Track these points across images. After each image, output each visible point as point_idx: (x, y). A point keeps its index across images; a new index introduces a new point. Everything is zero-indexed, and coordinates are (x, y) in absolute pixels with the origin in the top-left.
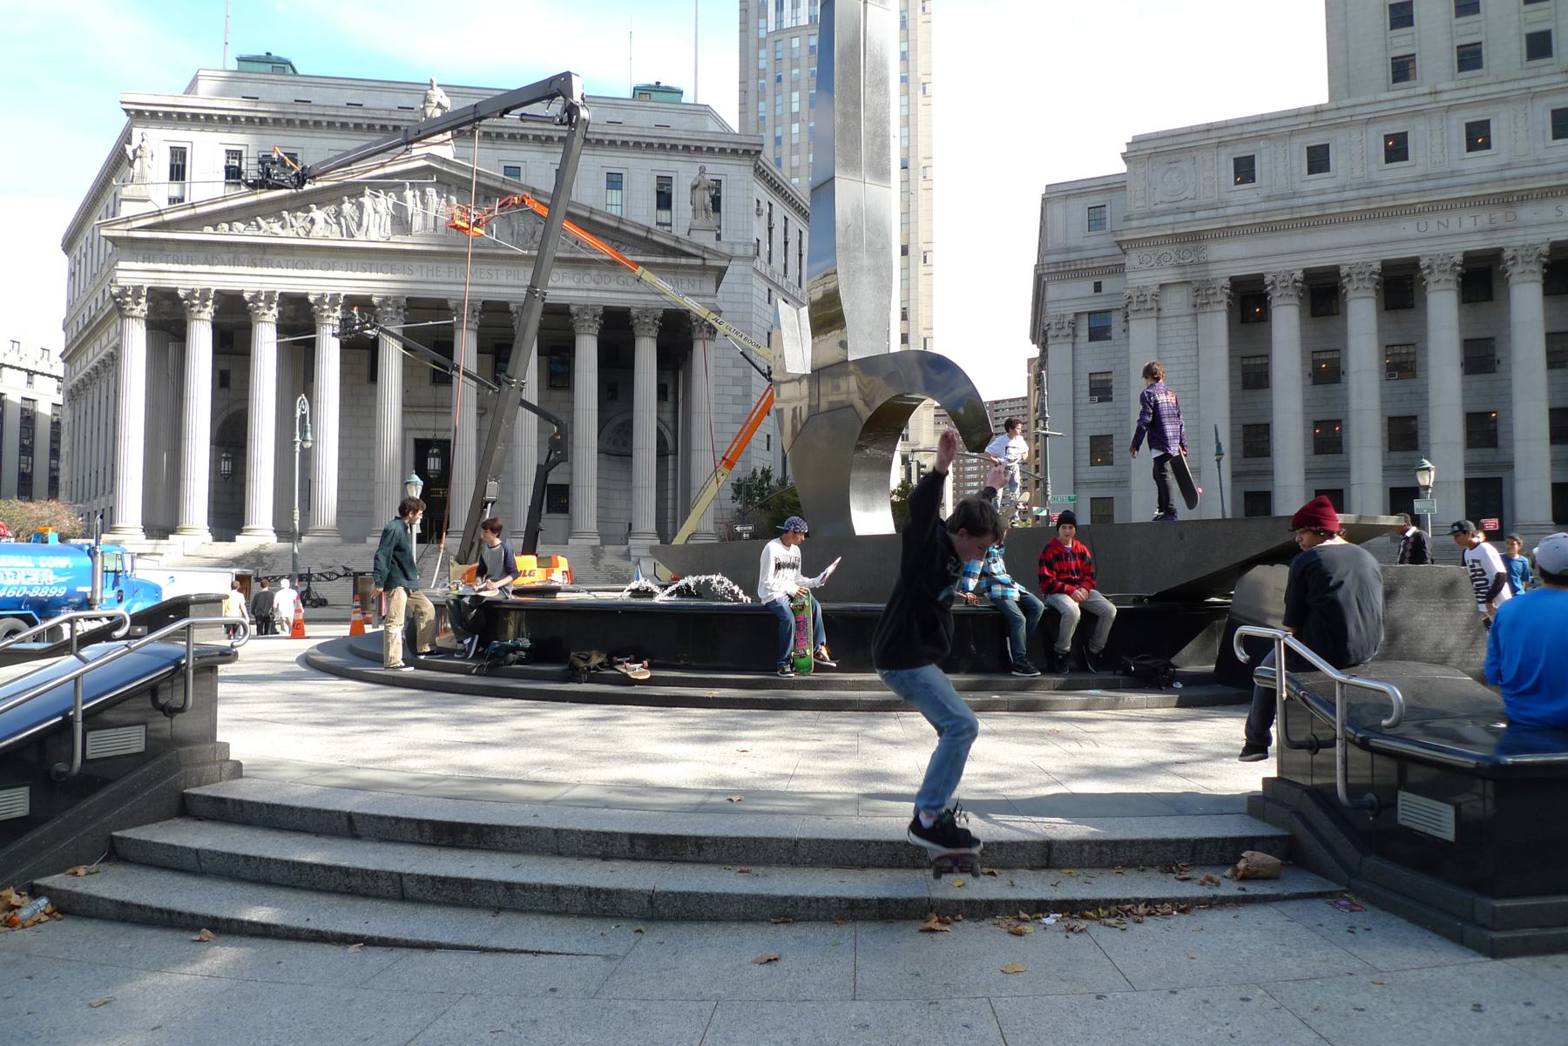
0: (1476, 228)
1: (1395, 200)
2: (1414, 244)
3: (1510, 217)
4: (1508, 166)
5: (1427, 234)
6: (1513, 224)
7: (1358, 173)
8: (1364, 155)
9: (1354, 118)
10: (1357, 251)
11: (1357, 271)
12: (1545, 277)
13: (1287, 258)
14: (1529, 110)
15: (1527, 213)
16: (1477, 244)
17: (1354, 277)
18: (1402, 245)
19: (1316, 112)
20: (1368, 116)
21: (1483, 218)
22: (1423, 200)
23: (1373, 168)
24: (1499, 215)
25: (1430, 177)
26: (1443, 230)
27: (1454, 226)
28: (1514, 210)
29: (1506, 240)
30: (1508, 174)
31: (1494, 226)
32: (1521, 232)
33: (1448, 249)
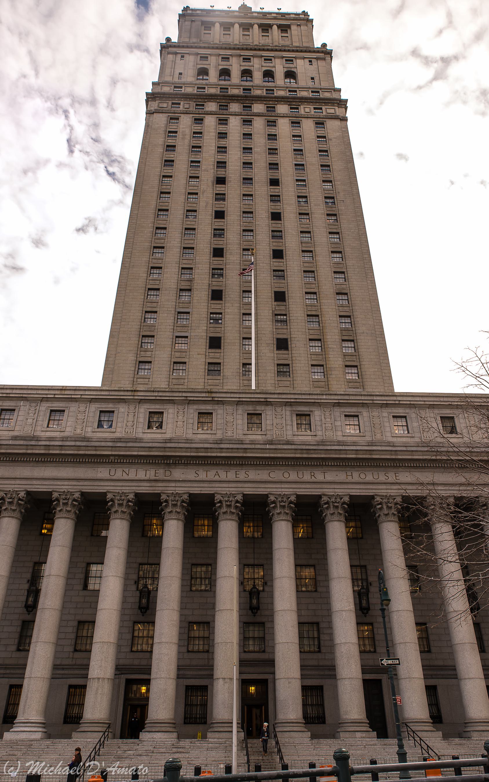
0: (146, 478)
1: (96, 450)
2: (106, 483)
3: (168, 473)
4: (170, 441)
5: (114, 478)
6: (169, 478)
7: (78, 431)
8: (85, 420)
9: (83, 397)
10: (66, 483)
11: (64, 497)
12: (186, 517)
13: (18, 482)
14: (186, 410)
15: (178, 473)
16: (145, 488)
17: (61, 501)
18: (96, 483)
19: (61, 390)
20: (92, 397)
21: (150, 473)
22: (114, 453)
23: (89, 429)
24: (161, 473)
25: (122, 440)
26: (125, 477)
27: (132, 476)
28: (171, 470)
29: (163, 488)
30: (169, 445)
31: (157, 478)
32: (173, 484)
33: (126, 489)
